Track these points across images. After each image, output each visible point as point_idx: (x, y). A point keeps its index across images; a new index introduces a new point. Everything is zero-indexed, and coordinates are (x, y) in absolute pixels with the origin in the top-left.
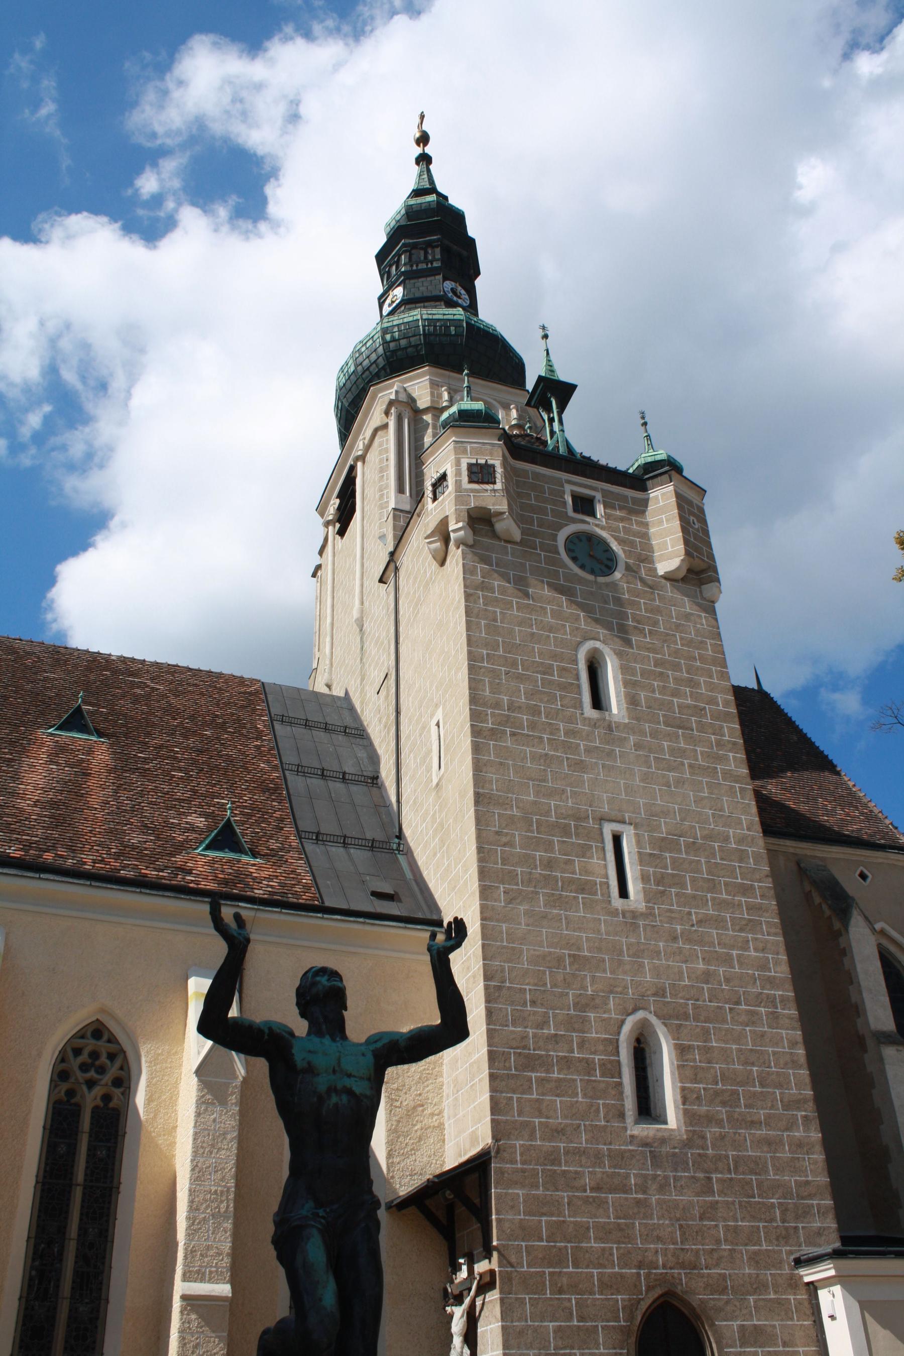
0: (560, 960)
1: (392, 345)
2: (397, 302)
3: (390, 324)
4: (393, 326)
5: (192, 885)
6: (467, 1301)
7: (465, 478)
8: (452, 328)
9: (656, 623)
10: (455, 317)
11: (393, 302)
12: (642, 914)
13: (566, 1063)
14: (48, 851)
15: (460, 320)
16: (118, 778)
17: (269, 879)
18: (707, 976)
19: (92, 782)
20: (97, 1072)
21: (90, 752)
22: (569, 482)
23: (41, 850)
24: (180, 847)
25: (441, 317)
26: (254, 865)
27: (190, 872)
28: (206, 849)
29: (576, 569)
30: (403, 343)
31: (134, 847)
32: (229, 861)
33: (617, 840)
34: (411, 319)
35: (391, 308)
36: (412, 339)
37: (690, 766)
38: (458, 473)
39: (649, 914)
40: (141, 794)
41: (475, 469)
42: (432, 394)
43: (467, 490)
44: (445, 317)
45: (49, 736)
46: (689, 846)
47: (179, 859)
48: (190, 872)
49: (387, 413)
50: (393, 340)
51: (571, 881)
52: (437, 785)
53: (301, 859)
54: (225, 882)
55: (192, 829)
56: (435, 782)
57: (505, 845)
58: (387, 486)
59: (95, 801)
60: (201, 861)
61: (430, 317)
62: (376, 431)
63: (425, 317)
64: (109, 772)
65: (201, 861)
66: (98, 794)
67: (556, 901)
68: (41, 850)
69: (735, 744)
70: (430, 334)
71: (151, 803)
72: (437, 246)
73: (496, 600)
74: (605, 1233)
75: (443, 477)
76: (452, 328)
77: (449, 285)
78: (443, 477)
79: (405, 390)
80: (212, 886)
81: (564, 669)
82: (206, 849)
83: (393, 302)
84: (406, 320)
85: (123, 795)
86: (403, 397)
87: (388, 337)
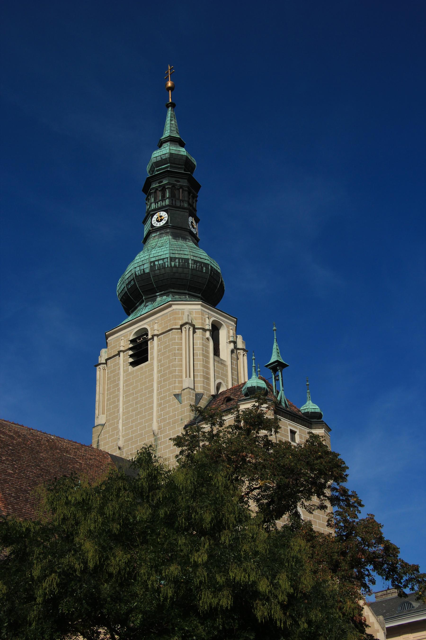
1: (174, 270)
4: (176, 258)
8: (204, 268)
22: (289, 425)
30: (180, 270)
50: (175, 266)
61: (195, 258)
70: (194, 269)
72: (186, 191)
76: (204, 268)
87: (173, 264)
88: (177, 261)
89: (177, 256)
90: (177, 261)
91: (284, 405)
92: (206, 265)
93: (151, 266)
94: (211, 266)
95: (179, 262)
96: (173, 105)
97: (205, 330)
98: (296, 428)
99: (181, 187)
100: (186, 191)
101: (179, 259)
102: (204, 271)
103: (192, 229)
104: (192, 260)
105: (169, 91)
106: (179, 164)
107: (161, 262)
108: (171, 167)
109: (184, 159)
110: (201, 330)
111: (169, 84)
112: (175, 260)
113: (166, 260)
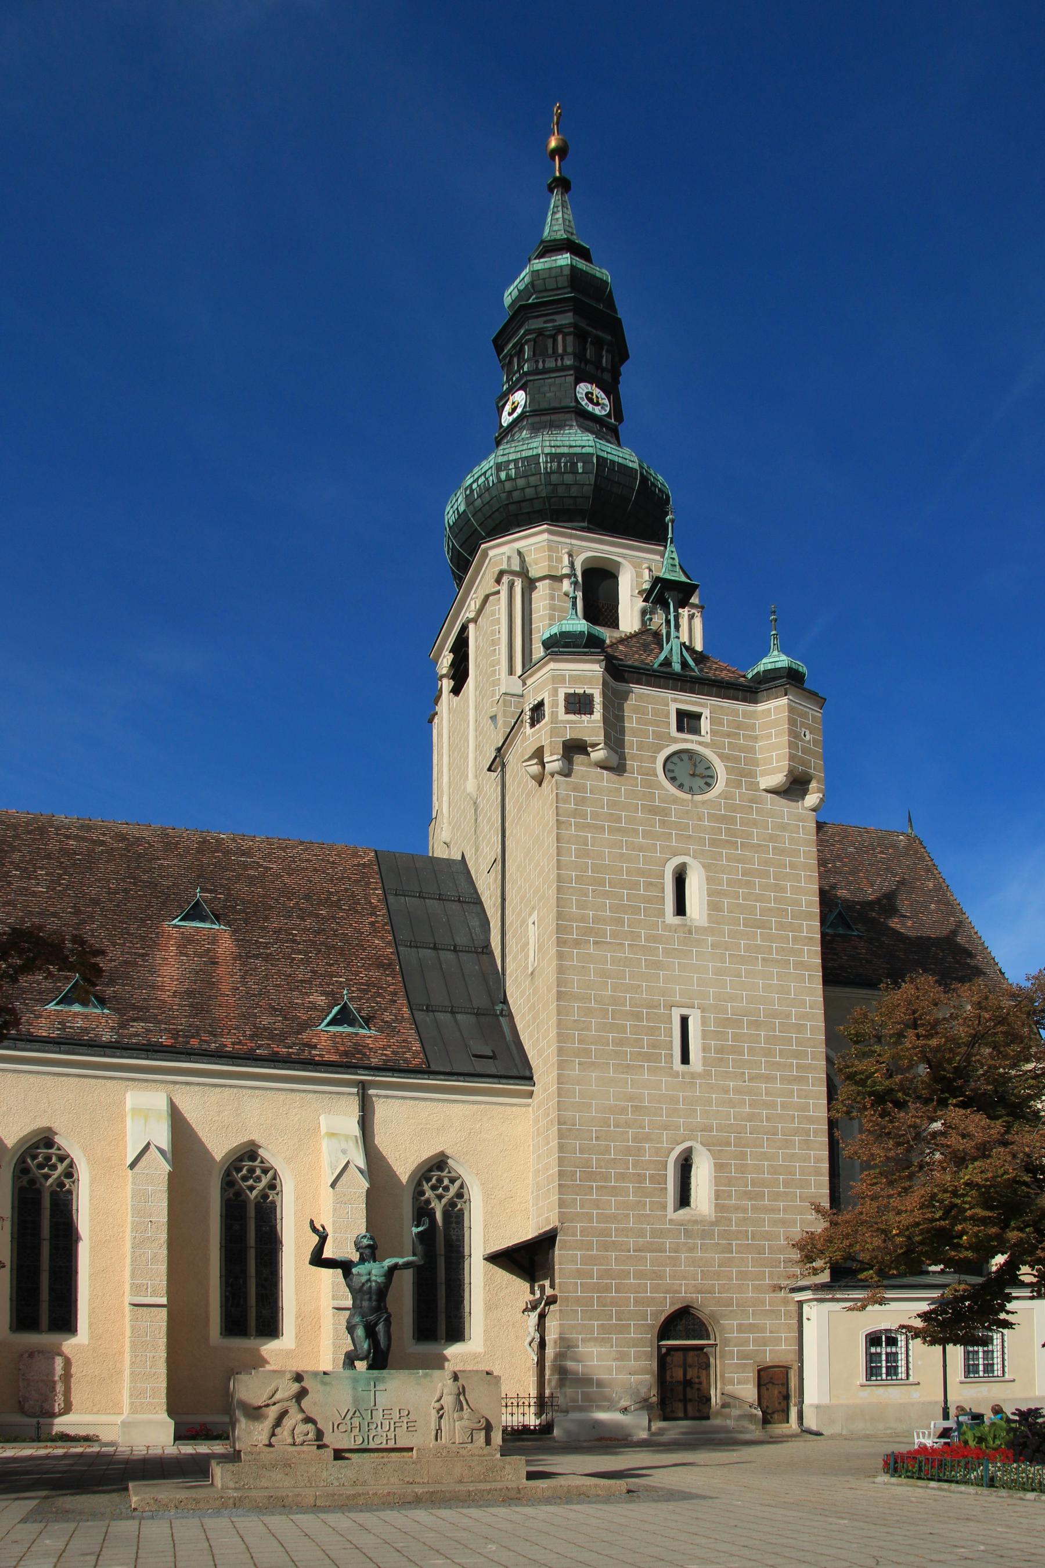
1: (508, 486)
2: (519, 410)
3: (505, 459)
4: (509, 462)
7: (561, 709)
8: (580, 465)
10: (584, 451)
11: (514, 410)
15: (589, 454)
16: (244, 964)
17: (384, 1048)
20: (255, 1181)
21: (214, 941)
24: (305, 1026)
25: (566, 450)
27: (315, 1047)
28: (328, 1025)
30: (521, 482)
32: (349, 1035)
33: (684, 1020)
34: (530, 453)
35: (511, 419)
36: (531, 479)
38: (555, 704)
40: (266, 978)
41: (572, 700)
42: (550, 558)
43: (563, 722)
44: (572, 450)
45: (176, 925)
47: (304, 1036)
49: (498, 581)
50: (509, 478)
52: (532, 973)
55: (314, 1007)
58: (499, 663)
60: (324, 1037)
62: (487, 598)
63: (547, 450)
64: (235, 959)
66: (227, 976)
70: (552, 472)
71: (276, 986)
72: (569, 334)
75: (541, 704)
76: (580, 465)
77: (583, 388)
78: (541, 704)
79: (519, 553)
82: (328, 1025)
83: (514, 410)
84: (524, 454)
86: (516, 567)
87: (503, 475)
88: (512, 466)
89: (512, 457)
90: (512, 466)
92: (585, 458)
93: (467, 496)
94: (598, 457)
95: (516, 468)
96: (563, 184)
97: (557, 579)
99: (559, 330)
100: (569, 334)
101: (516, 461)
102: (580, 471)
103: (590, 408)
104: (546, 455)
105: (554, 160)
106: (558, 289)
107: (481, 481)
108: (536, 298)
109: (567, 272)
110: (547, 581)
111: (553, 144)
112: (507, 469)
113: (489, 473)
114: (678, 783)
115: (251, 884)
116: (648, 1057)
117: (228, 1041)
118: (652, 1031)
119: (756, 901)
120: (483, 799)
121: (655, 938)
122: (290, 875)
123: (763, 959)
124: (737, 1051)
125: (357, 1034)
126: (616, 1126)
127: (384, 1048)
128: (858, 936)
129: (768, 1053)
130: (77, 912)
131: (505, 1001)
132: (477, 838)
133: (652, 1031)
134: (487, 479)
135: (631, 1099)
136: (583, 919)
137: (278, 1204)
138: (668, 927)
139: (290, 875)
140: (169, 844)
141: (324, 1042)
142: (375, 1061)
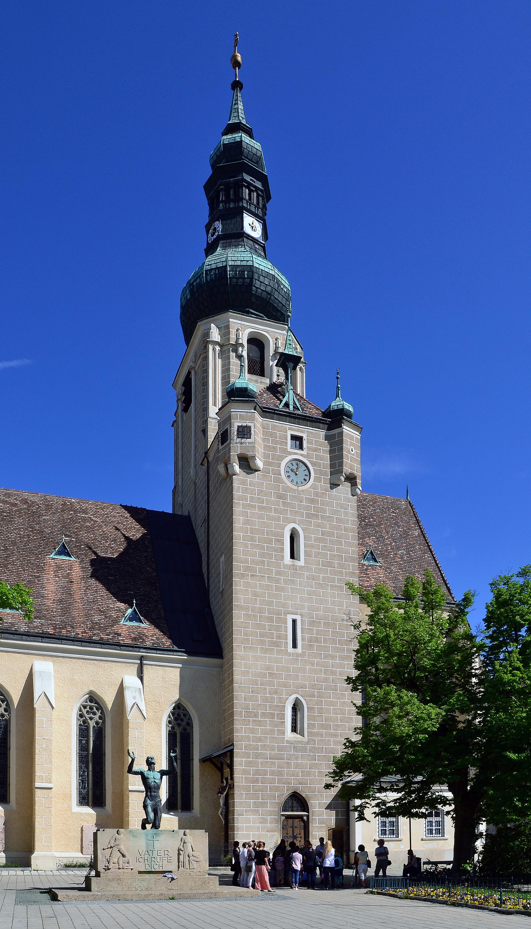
0: (265, 674)
5: (121, 642)
6: (225, 793)
9: (325, 511)
12: (300, 654)
13: (264, 715)
14: (63, 628)
17: (152, 636)
18: (326, 680)
19: (75, 586)
23: (60, 628)
26: (146, 629)
29: (289, 484)
31: (97, 623)
33: (294, 621)
37: (331, 586)
39: (303, 654)
40: (96, 591)
46: (325, 624)
48: (119, 635)
51: (272, 642)
53: (165, 624)
54: (134, 639)
56: (221, 590)
57: (245, 628)
59: (77, 597)
65: (125, 628)
67: (266, 651)
68: (60, 628)
69: (353, 573)
73: (249, 505)
74: (272, 773)
80: (128, 642)
81: (278, 540)
85: (88, 592)
91: (291, 407)
98: (302, 432)
114: (291, 479)
115: (88, 532)
116: (277, 644)
117: (79, 631)
118: (278, 628)
119: (328, 550)
120: (199, 480)
121: (279, 573)
122: (106, 526)
123: (331, 586)
124: (317, 640)
125: (139, 627)
126: (261, 685)
127: (152, 636)
128: (380, 567)
129: (334, 642)
130: (6, 549)
131: (209, 607)
132: (196, 504)
133: (278, 628)
134: (201, 280)
135: (268, 669)
136: (246, 561)
137: (103, 728)
138: (286, 566)
139: (106, 526)
140: (48, 505)
141: (124, 631)
142: (148, 644)
